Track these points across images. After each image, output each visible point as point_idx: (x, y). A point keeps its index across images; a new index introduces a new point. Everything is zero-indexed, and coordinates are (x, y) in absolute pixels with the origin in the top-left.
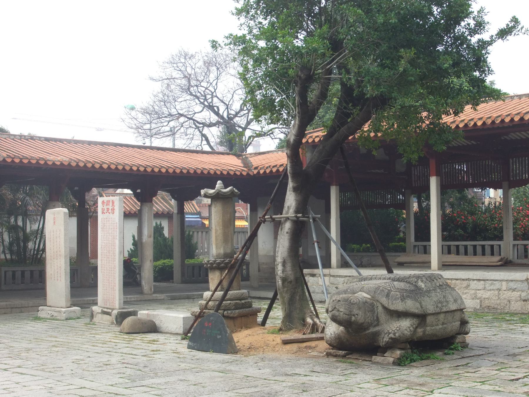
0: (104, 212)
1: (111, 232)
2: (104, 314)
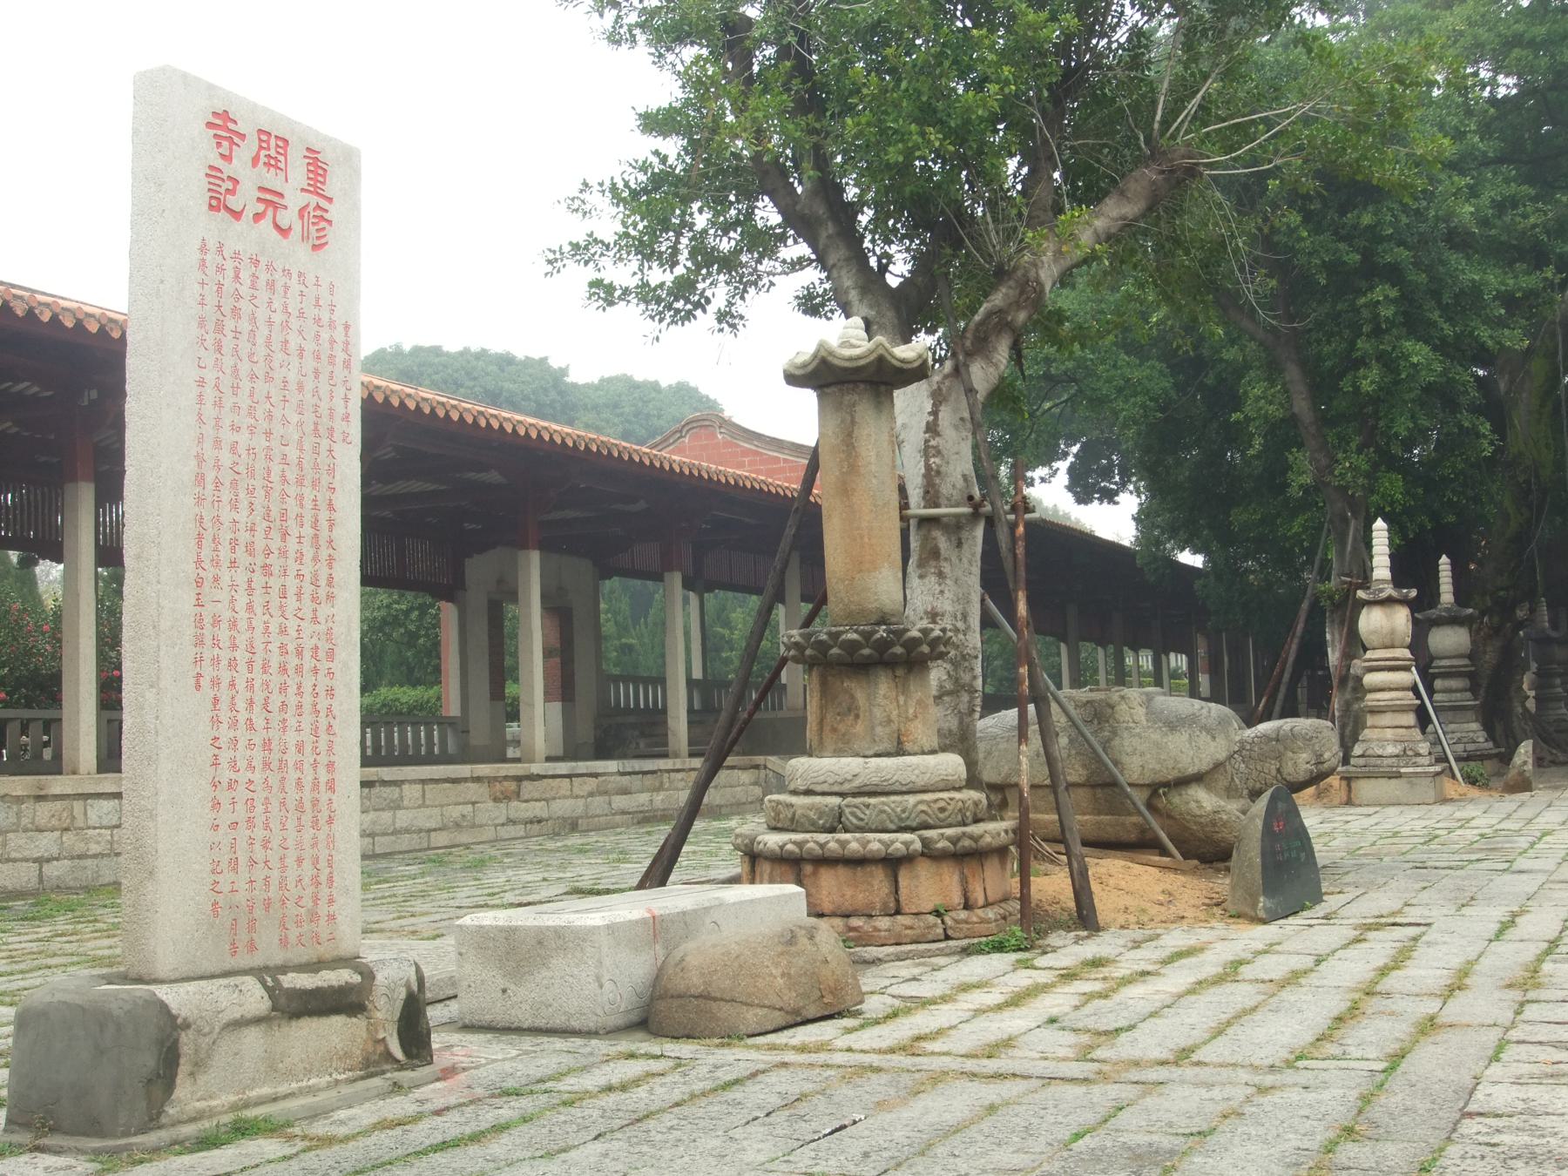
0: (234, 202)
1: (293, 377)
2: (297, 1015)
